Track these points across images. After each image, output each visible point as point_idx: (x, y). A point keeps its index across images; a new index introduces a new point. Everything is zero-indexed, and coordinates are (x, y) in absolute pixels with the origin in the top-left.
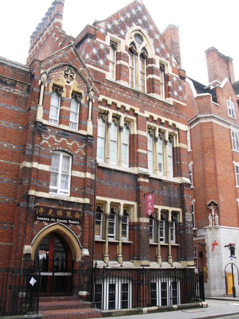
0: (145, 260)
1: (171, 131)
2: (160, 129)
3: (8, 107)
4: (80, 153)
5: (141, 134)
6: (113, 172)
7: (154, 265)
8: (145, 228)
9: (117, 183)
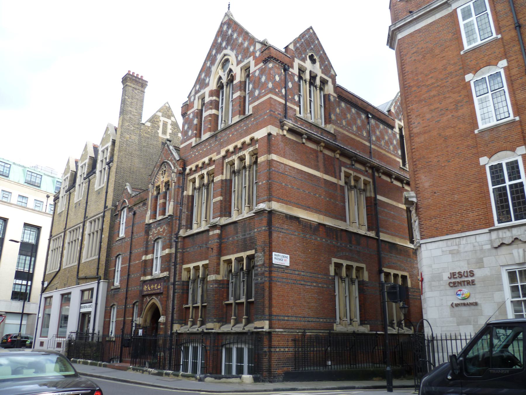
1: (251, 149)
2: (239, 157)
7: (226, 328)
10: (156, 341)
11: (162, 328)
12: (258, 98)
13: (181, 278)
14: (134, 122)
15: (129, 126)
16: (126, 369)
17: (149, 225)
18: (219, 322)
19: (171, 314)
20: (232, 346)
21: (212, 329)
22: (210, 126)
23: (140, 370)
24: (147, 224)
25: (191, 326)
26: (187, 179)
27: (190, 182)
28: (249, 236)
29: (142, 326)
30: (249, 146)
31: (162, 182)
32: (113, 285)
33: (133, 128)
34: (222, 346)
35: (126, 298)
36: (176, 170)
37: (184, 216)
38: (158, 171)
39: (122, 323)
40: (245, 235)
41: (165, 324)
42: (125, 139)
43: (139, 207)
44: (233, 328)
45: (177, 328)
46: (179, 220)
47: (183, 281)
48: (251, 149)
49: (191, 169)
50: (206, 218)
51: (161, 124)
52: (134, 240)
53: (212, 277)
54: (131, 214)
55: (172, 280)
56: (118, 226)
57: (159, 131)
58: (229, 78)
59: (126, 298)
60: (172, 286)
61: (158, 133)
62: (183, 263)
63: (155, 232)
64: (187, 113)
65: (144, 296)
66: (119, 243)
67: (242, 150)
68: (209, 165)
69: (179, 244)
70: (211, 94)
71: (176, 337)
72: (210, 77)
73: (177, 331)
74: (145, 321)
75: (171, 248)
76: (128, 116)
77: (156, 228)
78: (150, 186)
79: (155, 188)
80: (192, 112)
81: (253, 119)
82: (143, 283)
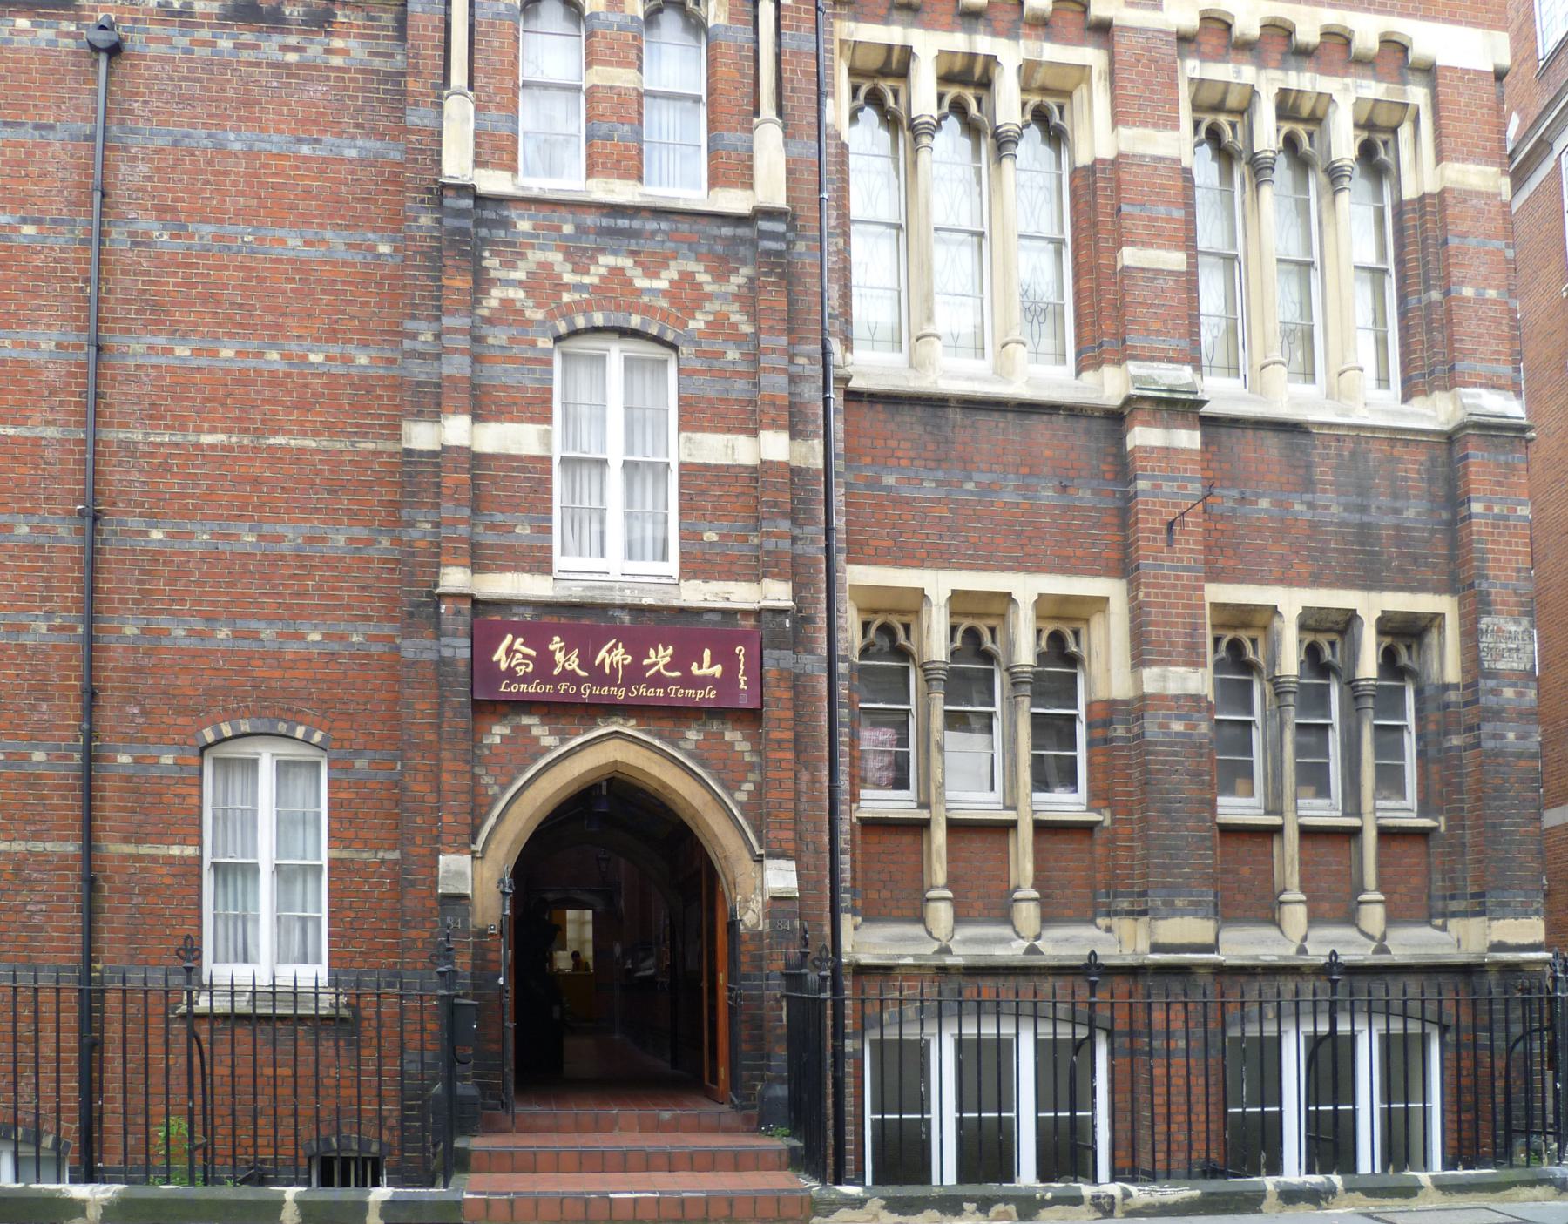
0: (1182, 913)
1: (1374, 89)
2: (1284, 93)
3: (305, 150)
4: (719, 325)
5: (1140, 149)
6: (954, 415)
8: (1177, 726)
9: (985, 478)
30: (1360, 69)
39: (72, 879)
53: (1185, 679)
59: (91, 696)
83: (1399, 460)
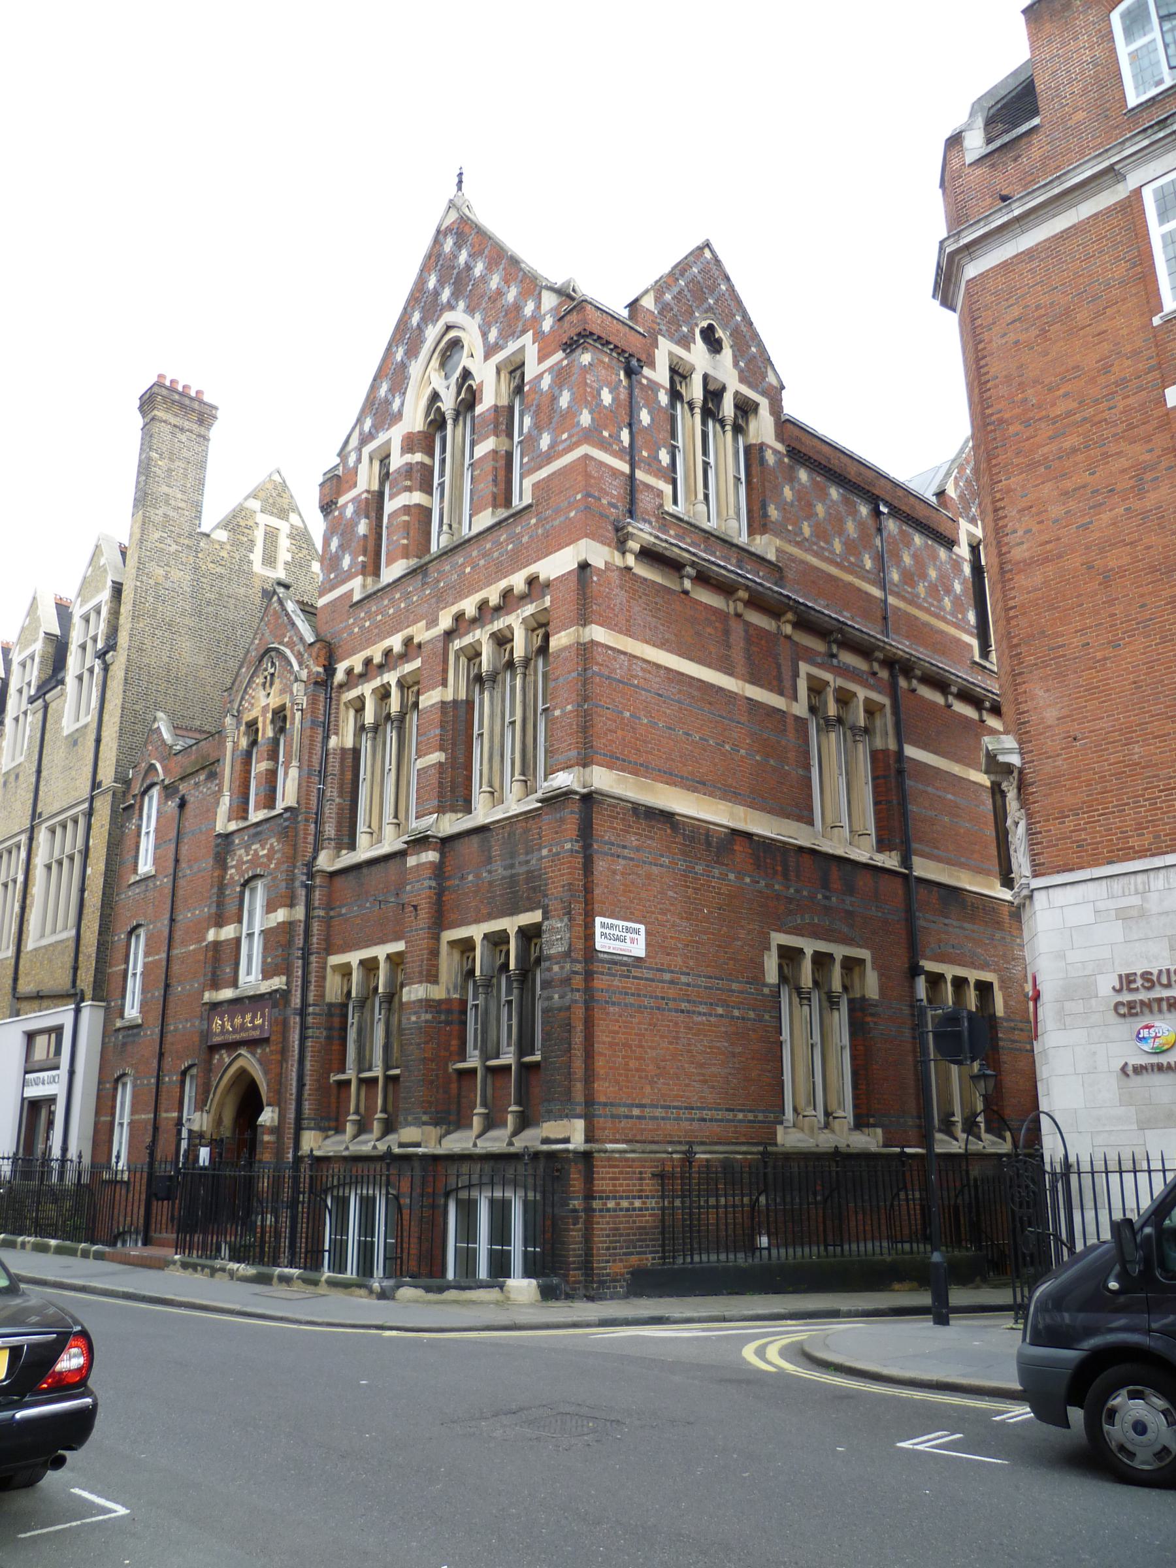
1: (529, 609)
2: (493, 635)
7: (458, 1142)
8: (413, 1018)
10: (250, 1183)
11: (268, 1142)
12: (549, 457)
13: (323, 996)
14: (177, 530)
15: (161, 540)
16: (161, 1265)
17: (227, 837)
18: (436, 1123)
19: (294, 1103)
20: (475, 1194)
21: (418, 1145)
22: (405, 542)
23: (203, 1267)
24: (219, 835)
25: (355, 1137)
26: (338, 701)
27: (347, 708)
28: (524, 869)
29: (208, 1136)
30: (524, 601)
31: (265, 709)
32: (122, 1016)
33: (174, 547)
34: (447, 1195)
35: (161, 1055)
36: (304, 674)
37: (330, 811)
38: (252, 677)
39: (150, 1128)
40: (512, 866)
41: (277, 1130)
42: (150, 581)
43: (196, 784)
44: (478, 1141)
45: (312, 1142)
46: (316, 823)
47: (330, 1005)
48: (529, 609)
49: (349, 672)
50: (396, 817)
51: (259, 535)
52: (182, 882)
53: (417, 991)
54: (172, 804)
55: (296, 1001)
56: (133, 841)
57: (252, 557)
58: (463, 395)
59: (161, 1055)
60: (298, 1019)
61: (250, 562)
62: (329, 950)
63: (245, 859)
64: (336, 503)
65: (213, 1049)
66: (137, 891)
67: (502, 612)
68: (404, 657)
69: (317, 894)
70: (409, 444)
71: (311, 1170)
72: (404, 393)
73: (312, 1151)
74: (219, 1122)
75: (291, 905)
76: (160, 512)
77: (247, 848)
78: (228, 720)
79: (243, 728)
80: (353, 500)
81: (533, 521)
82: (210, 1010)
83: (530, 830)
